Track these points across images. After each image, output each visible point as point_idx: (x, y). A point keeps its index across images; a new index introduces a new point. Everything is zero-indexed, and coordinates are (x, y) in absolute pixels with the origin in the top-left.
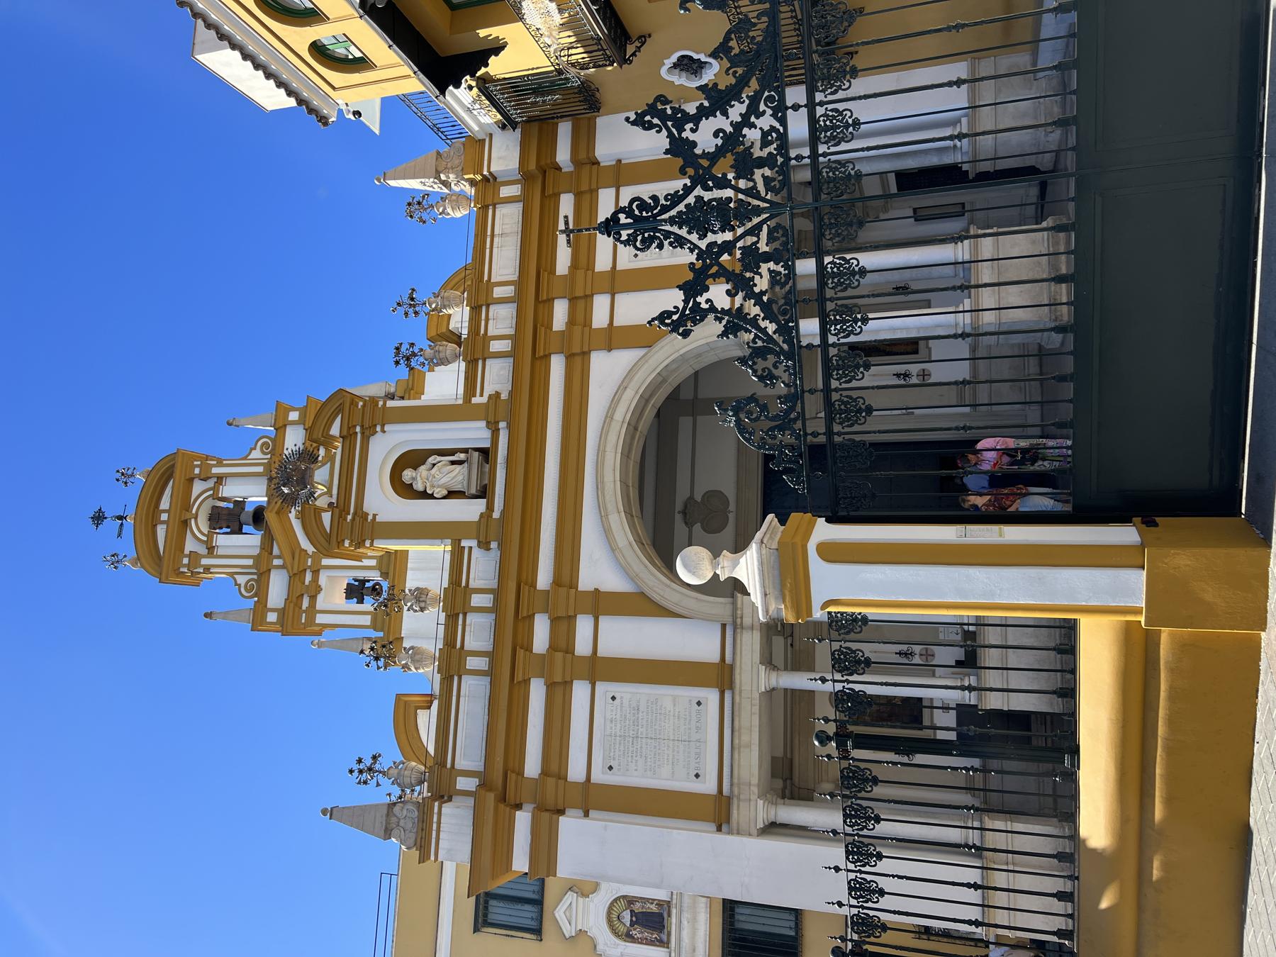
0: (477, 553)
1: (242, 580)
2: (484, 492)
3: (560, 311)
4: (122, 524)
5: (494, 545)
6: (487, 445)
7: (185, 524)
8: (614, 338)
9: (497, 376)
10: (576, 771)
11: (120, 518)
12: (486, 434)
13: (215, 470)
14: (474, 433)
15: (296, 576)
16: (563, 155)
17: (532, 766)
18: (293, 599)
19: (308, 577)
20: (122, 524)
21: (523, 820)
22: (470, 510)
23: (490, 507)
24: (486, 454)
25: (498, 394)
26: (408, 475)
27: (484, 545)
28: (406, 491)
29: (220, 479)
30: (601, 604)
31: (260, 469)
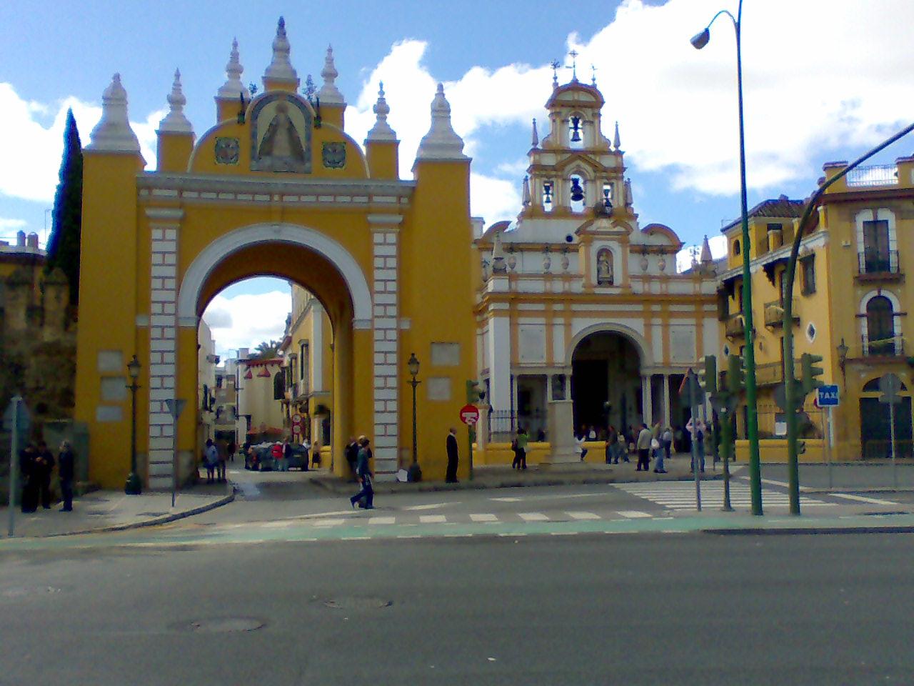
0: (581, 283)
1: (550, 139)
2: (600, 283)
3: (656, 308)
4: (571, 68)
5: (583, 289)
6: (615, 283)
7: (573, 107)
8: (648, 326)
9: (638, 287)
10: (522, 320)
11: (574, 66)
12: (618, 284)
13: (596, 121)
14: (618, 280)
15: (554, 168)
16: (707, 308)
17: (521, 307)
18: (544, 168)
19: (554, 173)
20: (571, 68)
21: (506, 306)
22: (594, 281)
23: (595, 287)
24: (611, 283)
25: (630, 287)
26: (604, 254)
27: (584, 286)
28: (600, 254)
29: (592, 123)
30: (568, 326)
31: (597, 144)
